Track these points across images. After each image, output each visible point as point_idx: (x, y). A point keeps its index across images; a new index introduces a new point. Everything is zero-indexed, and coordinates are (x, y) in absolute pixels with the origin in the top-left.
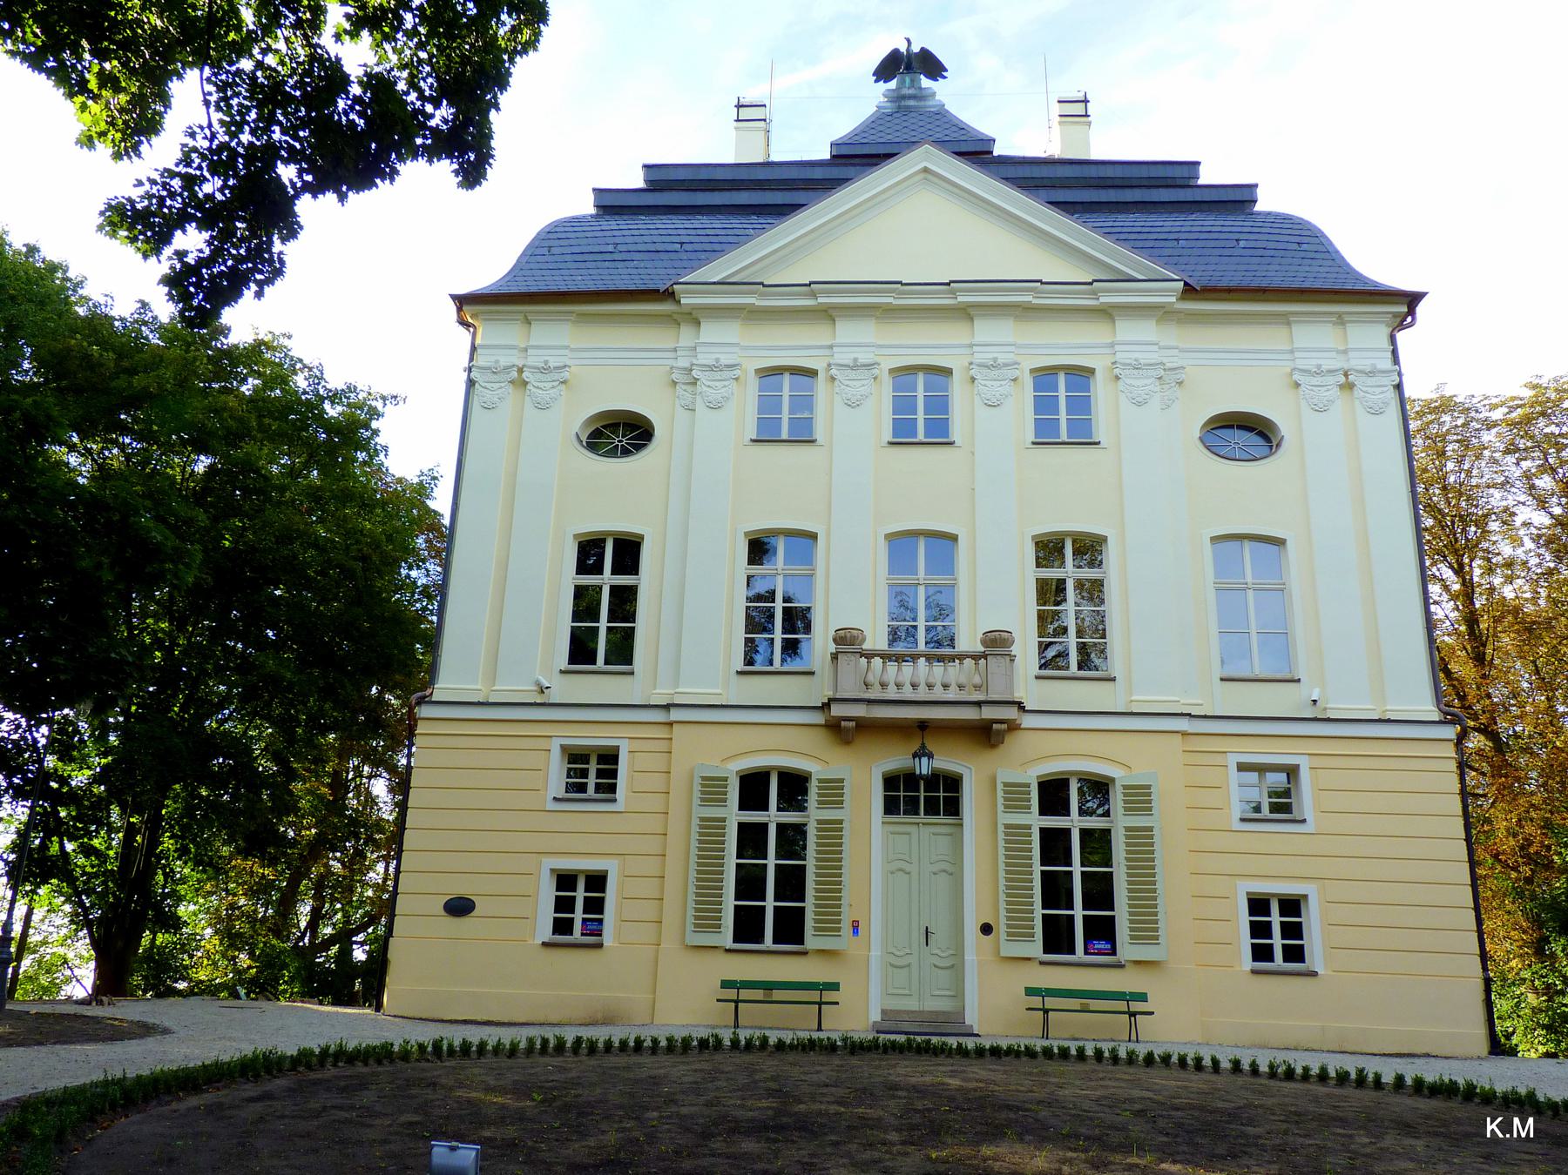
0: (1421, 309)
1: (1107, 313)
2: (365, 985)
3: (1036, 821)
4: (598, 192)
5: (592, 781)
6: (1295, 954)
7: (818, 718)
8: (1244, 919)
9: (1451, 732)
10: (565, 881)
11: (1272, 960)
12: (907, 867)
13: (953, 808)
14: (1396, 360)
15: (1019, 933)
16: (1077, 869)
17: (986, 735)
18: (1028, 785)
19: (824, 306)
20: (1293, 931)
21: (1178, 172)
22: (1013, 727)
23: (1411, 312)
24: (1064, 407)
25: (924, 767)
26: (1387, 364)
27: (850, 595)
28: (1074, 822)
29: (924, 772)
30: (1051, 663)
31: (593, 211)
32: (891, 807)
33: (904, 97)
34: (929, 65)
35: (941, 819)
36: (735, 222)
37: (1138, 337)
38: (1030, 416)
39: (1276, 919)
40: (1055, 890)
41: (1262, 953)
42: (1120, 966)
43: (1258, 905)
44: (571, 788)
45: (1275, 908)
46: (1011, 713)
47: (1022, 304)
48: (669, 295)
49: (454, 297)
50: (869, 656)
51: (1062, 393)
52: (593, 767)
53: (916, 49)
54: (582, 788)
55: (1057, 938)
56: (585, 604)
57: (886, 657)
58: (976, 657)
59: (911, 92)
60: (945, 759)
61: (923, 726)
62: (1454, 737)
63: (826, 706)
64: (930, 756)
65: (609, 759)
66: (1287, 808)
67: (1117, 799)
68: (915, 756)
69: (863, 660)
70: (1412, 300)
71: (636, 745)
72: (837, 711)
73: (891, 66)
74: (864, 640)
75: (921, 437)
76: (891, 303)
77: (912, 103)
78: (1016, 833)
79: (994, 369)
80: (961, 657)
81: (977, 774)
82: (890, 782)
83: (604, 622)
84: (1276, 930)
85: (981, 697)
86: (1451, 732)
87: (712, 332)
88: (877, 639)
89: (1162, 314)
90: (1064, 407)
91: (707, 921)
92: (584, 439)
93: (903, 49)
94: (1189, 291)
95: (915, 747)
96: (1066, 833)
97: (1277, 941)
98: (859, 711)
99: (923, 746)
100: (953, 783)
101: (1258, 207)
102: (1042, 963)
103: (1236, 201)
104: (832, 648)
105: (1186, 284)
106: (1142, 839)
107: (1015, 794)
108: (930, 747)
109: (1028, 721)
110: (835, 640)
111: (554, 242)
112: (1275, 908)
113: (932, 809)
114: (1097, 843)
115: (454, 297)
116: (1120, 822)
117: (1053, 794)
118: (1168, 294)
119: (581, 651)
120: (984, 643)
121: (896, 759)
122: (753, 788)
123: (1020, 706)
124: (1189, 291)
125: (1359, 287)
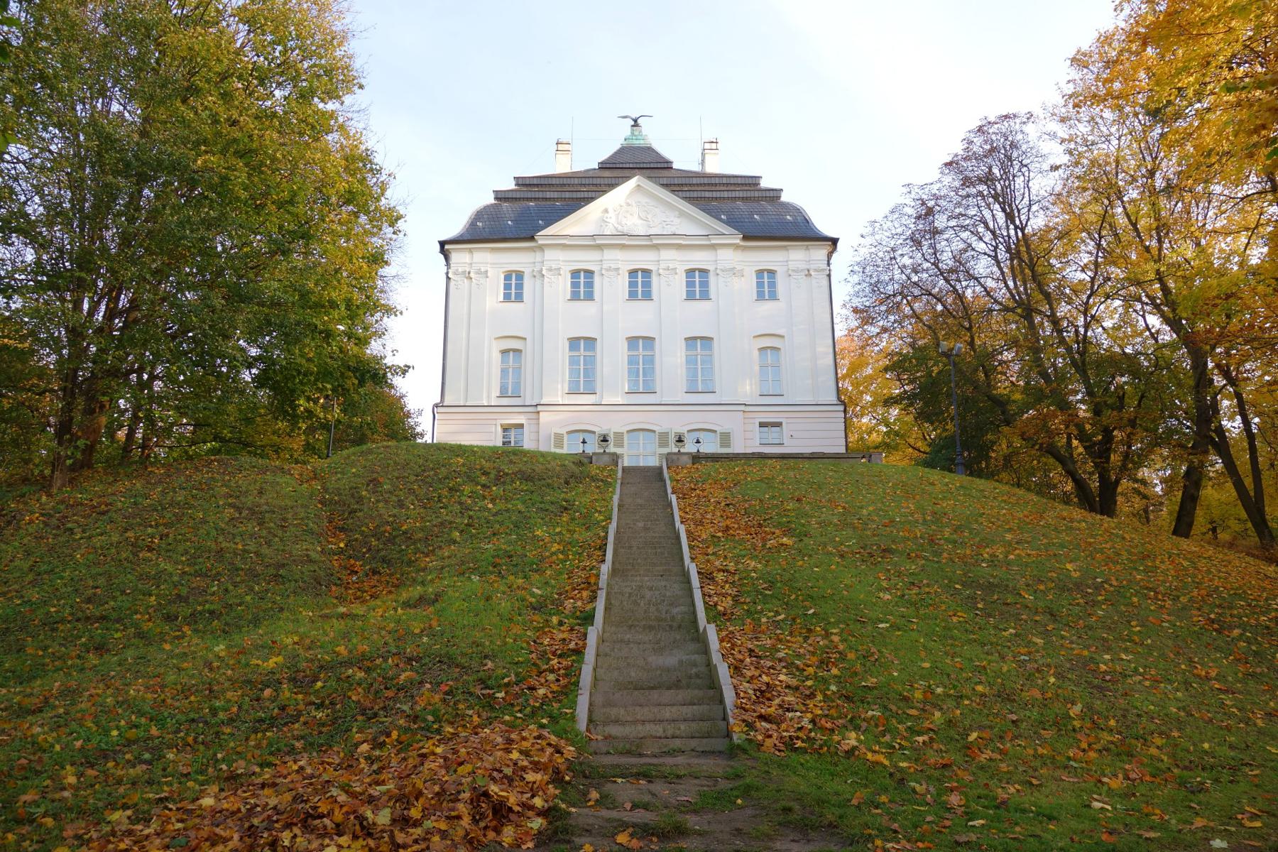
0: (839, 244)
1: (713, 247)
4: (496, 192)
9: (842, 408)
14: (829, 264)
19: (595, 243)
24: (698, 284)
26: (825, 266)
31: (493, 201)
37: (728, 257)
38: (684, 289)
47: (679, 244)
48: (532, 238)
51: (697, 279)
70: (834, 242)
76: (625, 241)
79: (670, 269)
87: (550, 255)
89: (737, 247)
90: (698, 284)
94: (745, 238)
111: (479, 215)
118: (737, 240)
125: (810, 234)
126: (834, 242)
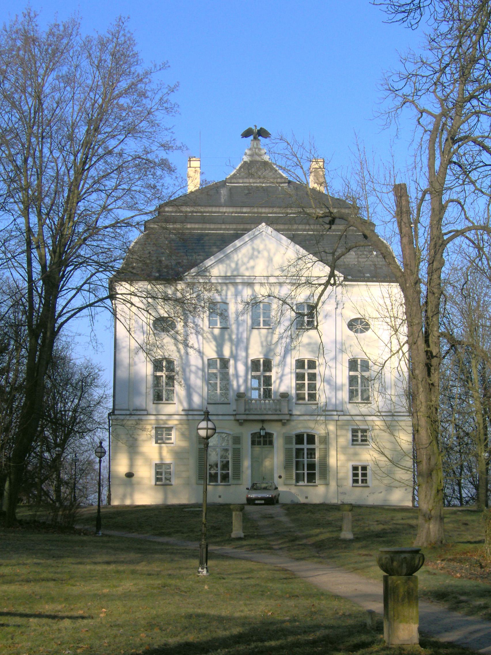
3: (295, 446)
6: (364, 481)
7: (232, 418)
13: (271, 443)
20: (364, 475)
32: (253, 443)
34: (262, 133)
35: (268, 446)
39: (360, 472)
41: (355, 481)
43: (355, 468)
53: (258, 128)
61: (263, 421)
68: (261, 429)
72: (238, 417)
78: (288, 452)
81: (277, 432)
82: (253, 435)
84: (360, 475)
85: (279, 413)
93: (254, 128)
96: (303, 449)
98: (244, 417)
113: (265, 443)
116: (318, 446)
117: (299, 438)
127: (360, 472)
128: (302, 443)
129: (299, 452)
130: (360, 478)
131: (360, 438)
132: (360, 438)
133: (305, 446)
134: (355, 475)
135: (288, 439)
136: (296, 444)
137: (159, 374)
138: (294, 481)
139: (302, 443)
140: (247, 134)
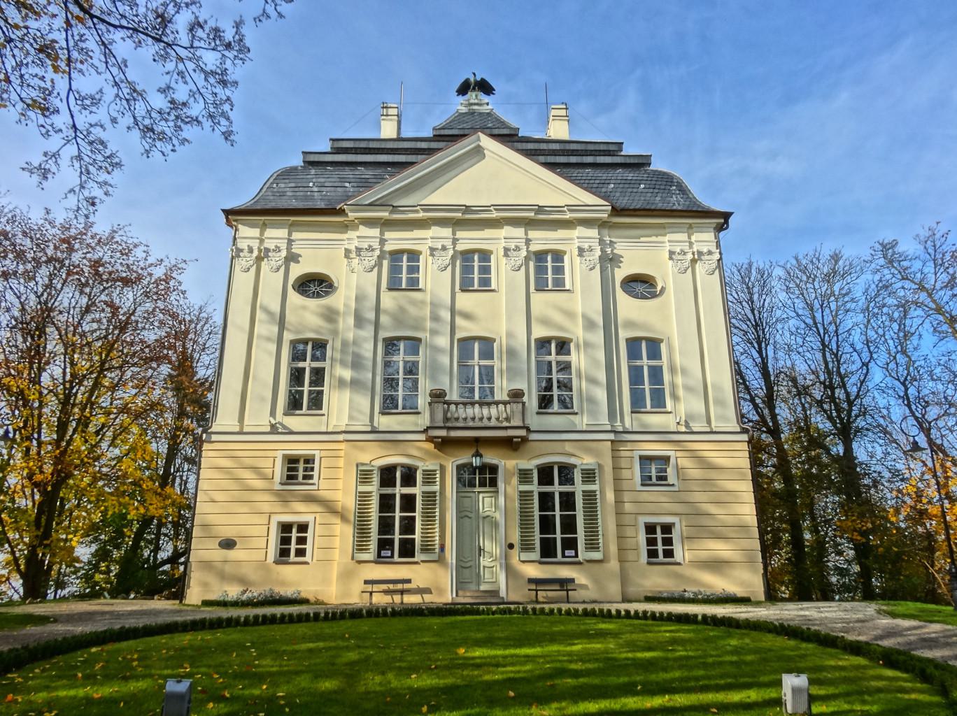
2: (176, 588)
3: (535, 488)
5: (301, 473)
7: (423, 437)
8: (642, 537)
9: (745, 437)
10: (286, 528)
11: (658, 557)
12: (470, 515)
13: (493, 483)
15: (526, 547)
16: (558, 513)
17: (511, 445)
18: (531, 470)
21: (612, 148)
22: (524, 440)
23: (726, 222)
25: (476, 462)
27: (439, 369)
28: (557, 488)
29: (478, 465)
30: (545, 402)
33: (472, 104)
36: (378, 171)
39: (659, 536)
40: (547, 525)
41: (652, 554)
42: (579, 563)
44: (289, 477)
45: (659, 530)
46: (523, 433)
49: (224, 211)
50: (449, 403)
52: (301, 466)
53: (478, 79)
54: (295, 477)
55: (548, 550)
56: (297, 376)
57: (457, 404)
58: (505, 403)
59: (476, 101)
60: (490, 457)
62: (747, 439)
63: (425, 431)
64: (481, 456)
65: (309, 460)
66: (665, 478)
67: (578, 477)
69: (446, 406)
70: (726, 216)
71: (323, 454)
73: (464, 89)
74: (446, 395)
75: (476, 287)
77: (476, 107)
80: (497, 403)
83: (304, 389)
84: (660, 542)
85: (507, 424)
86: (745, 437)
88: (454, 396)
91: (360, 546)
92: (296, 288)
93: (472, 80)
95: (473, 451)
97: (660, 547)
98: (443, 433)
99: (477, 451)
100: (494, 469)
101: (652, 167)
102: (541, 563)
103: (640, 164)
104: (429, 399)
105: (612, 207)
106: (590, 497)
107: (524, 476)
108: (481, 451)
109: (533, 436)
110: (430, 395)
112: (659, 530)
113: (482, 484)
114: (568, 501)
115: (224, 211)
116: (579, 488)
117: (545, 474)
119: (294, 404)
120: (508, 395)
121: (465, 457)
122: (387, 474)
123: (528, 429)
124: (616, 211)
125: (699, 209)
126: (726, 216)
127: (659, 536)
128: (551, 483)
129: (546, 500)
130: (660, 547)
131: (654, 474)
132: (654, 474)
133: (557, 488)
134: (651, 542)
135: (524, 476)
136: (540, 483)
137: (301, 365)
138: (536, 555)
139: (551, 483)
140: (464, 89)
